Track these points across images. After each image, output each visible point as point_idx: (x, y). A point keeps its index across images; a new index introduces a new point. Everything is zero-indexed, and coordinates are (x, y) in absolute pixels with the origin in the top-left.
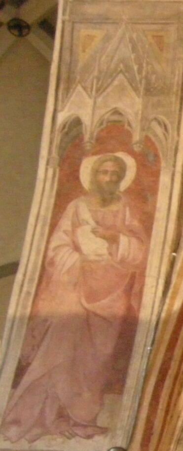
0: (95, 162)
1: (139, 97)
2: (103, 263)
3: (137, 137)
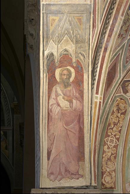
0: (60, 71)
1: (74, 44)
3: (74, 60)
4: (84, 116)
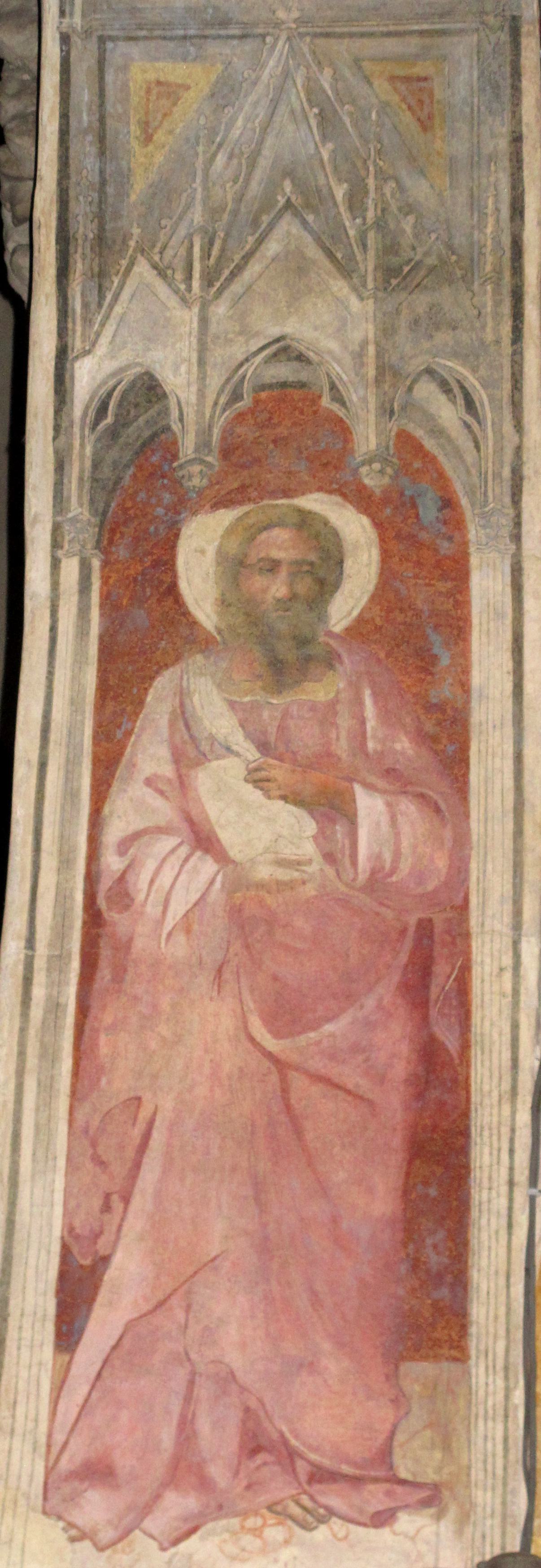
0: (230, 531)
1: (361, 298)
2: (310, 890)
4: (467, 936)
